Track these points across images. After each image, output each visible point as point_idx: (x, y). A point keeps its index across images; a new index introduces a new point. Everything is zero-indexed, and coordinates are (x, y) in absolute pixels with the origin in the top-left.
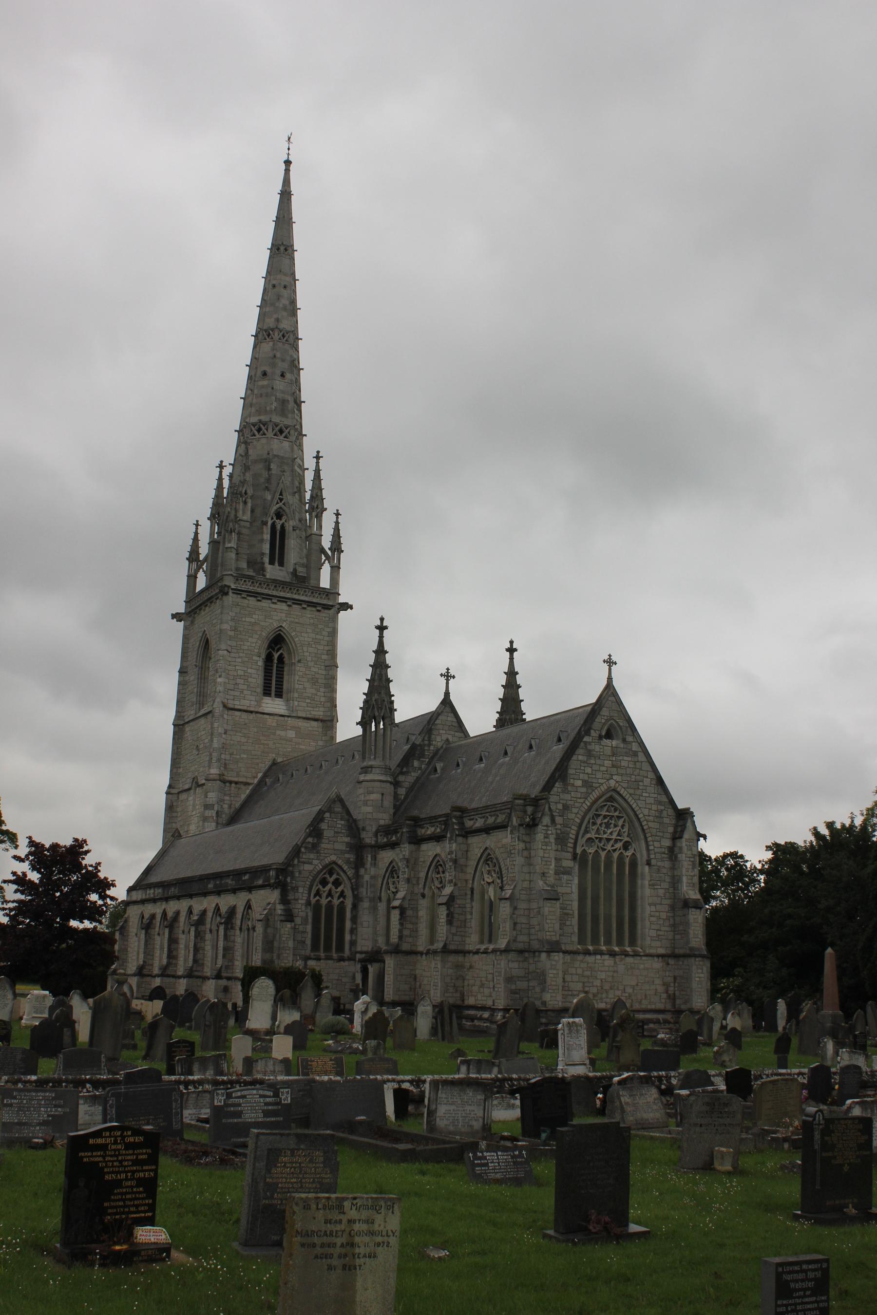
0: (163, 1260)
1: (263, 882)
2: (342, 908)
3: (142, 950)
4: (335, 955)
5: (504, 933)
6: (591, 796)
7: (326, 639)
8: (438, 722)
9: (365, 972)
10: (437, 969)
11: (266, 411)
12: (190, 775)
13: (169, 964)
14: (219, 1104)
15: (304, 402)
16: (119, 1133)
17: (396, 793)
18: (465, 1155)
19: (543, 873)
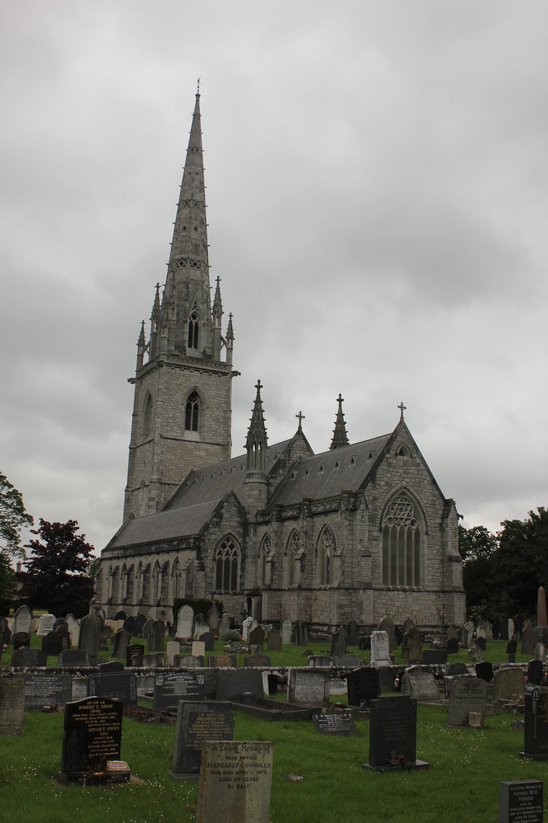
0: (125, 781)
2: (235, 563)
3: (111, 589)
4: (231, 592)
5: (336, 577)
6: (391, 491)
7: (224, 394)
8: (294, 445)
9: (250, 602)
10: (294, 600)
11: (186, 251)
12: (140, 480)
13: (127, 597)
14: (159, 684)
15: (209, 246)
16: (97, 703)
17: (268, 490)
18: (313, 716)
19: (361, 540)
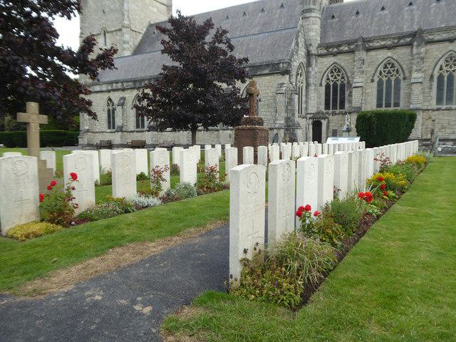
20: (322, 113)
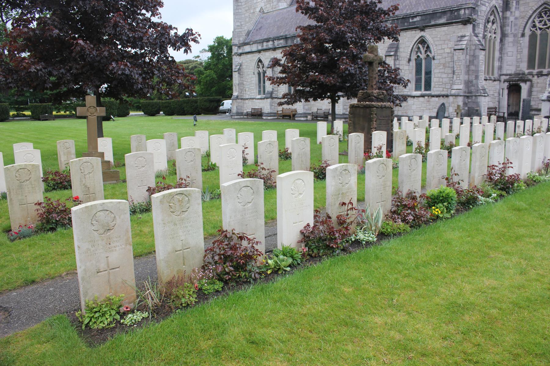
1: (447, 21)
20: (524, 74)
